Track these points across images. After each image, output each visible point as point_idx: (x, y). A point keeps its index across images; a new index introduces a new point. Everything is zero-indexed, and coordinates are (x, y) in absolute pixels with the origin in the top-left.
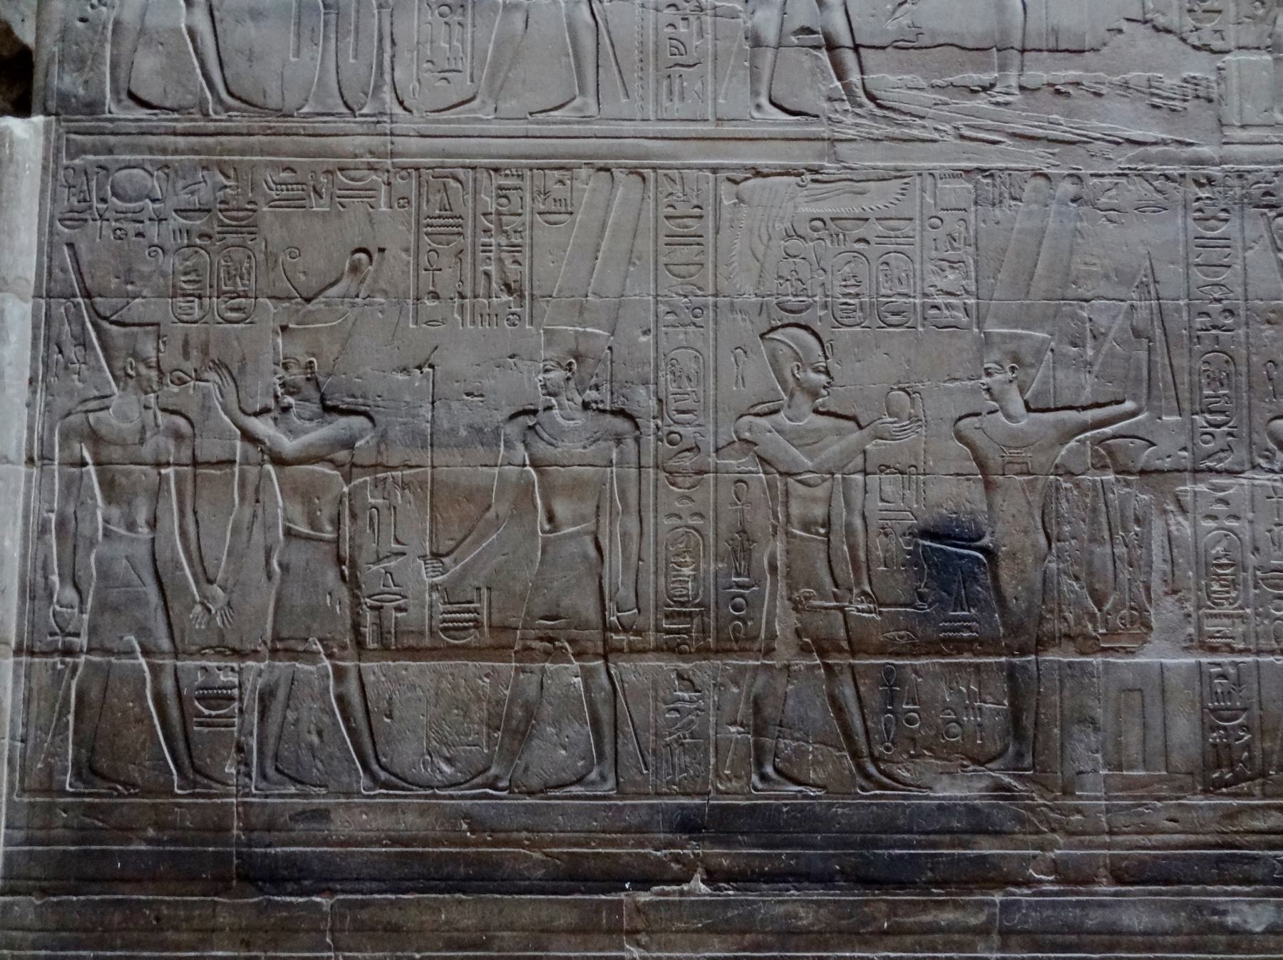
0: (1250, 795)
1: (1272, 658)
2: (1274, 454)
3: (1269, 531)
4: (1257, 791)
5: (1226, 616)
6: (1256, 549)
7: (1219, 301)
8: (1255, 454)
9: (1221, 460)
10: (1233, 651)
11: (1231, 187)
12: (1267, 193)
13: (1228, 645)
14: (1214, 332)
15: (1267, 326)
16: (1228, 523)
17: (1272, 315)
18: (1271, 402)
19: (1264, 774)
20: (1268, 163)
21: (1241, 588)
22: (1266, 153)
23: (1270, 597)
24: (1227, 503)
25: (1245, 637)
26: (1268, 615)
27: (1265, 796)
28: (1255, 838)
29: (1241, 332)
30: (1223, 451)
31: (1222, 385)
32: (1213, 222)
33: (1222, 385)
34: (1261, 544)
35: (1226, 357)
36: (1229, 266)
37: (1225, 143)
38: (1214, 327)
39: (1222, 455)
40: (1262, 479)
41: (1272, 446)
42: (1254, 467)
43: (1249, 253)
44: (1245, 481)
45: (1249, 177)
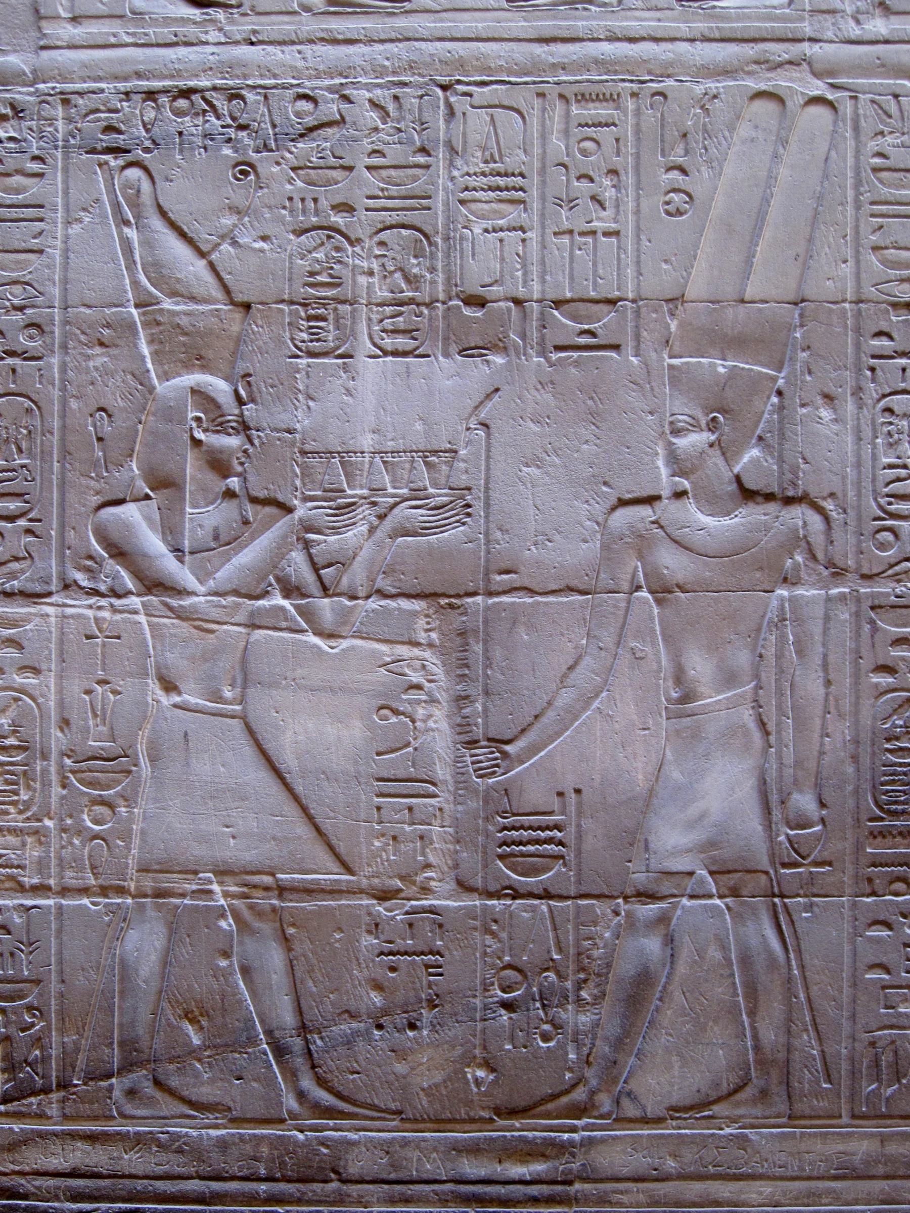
0: (41, 1116)
1: (86, 901)
2: (100, 563)
3: (88, 692)
4: (54, 1111)
5: (13, 831)
6: (65, 723)
7: (21, 309)
8: (69, 565)
9: (13, 576)
10: (21, 888)
11: (51, 120)
12: (110, 129)
13: (11, 878)
14: (10, 361)
15: (98, 350)
16: (19, 680)
17: (106, 332)
18: (100, 477)
19: (63, 1085)
20: (116, 78)
21: (38, 785)
22: (110, 60)
23: (85, 800)
24: (20, 647)
25: (41, 866)
26: (80, 831)
27: (66, 1118)
28: (51, 1182)
29: (55, 361)
30: (17, 559)
31: (20, 450)
32: (18, 179)
33: (20, 450)
34: (74, 717)
35: (28, 403)
36: (41, 252)
37: (43, 48)
38: (12, 354)
39: (15, 566)
40: (80, 607)
41: (98, 548)
42: (67, 586)
43: (75, 229)
44: (50, 610)
45: (81, 101)
